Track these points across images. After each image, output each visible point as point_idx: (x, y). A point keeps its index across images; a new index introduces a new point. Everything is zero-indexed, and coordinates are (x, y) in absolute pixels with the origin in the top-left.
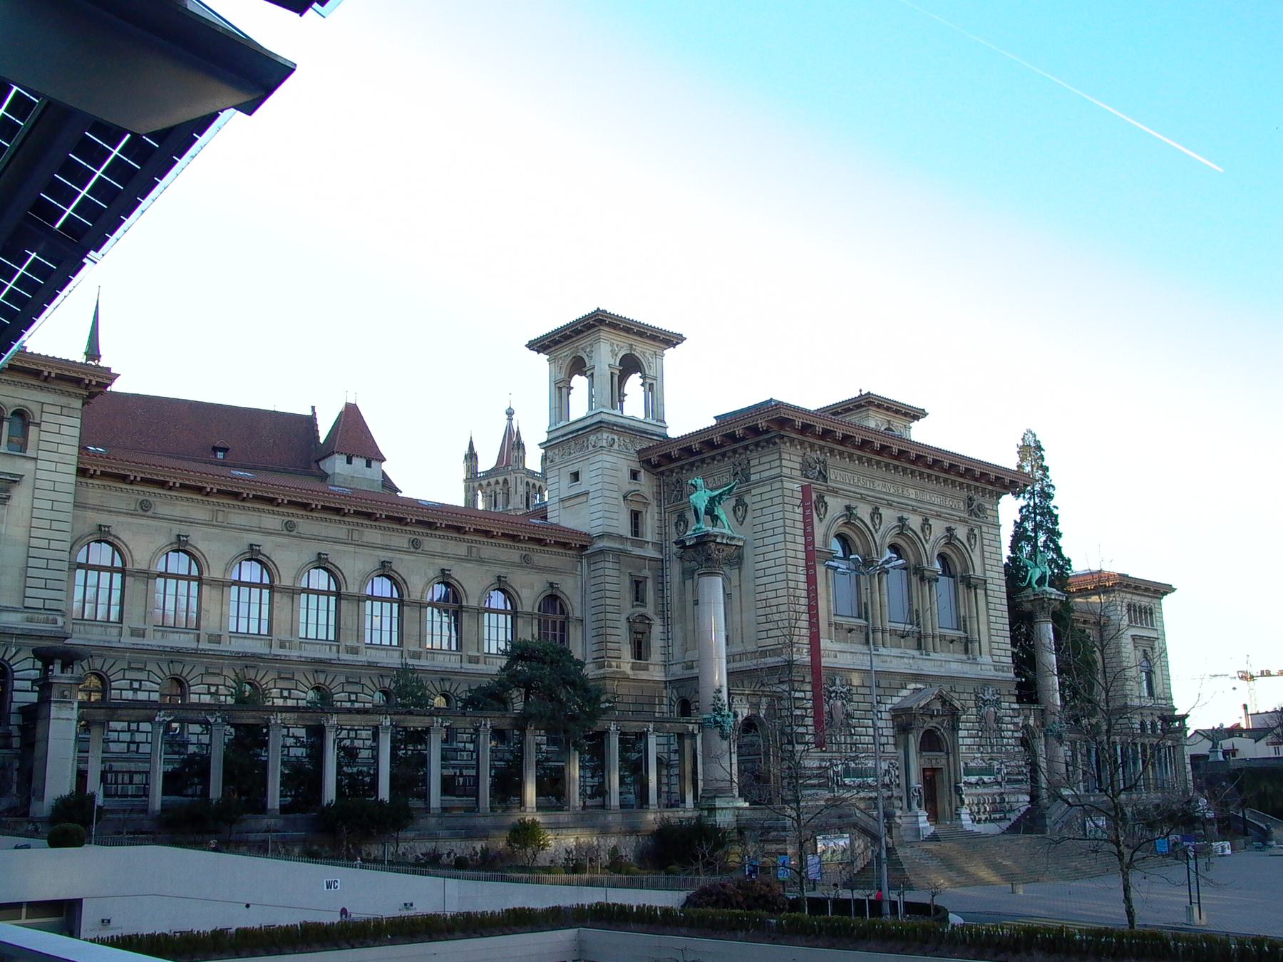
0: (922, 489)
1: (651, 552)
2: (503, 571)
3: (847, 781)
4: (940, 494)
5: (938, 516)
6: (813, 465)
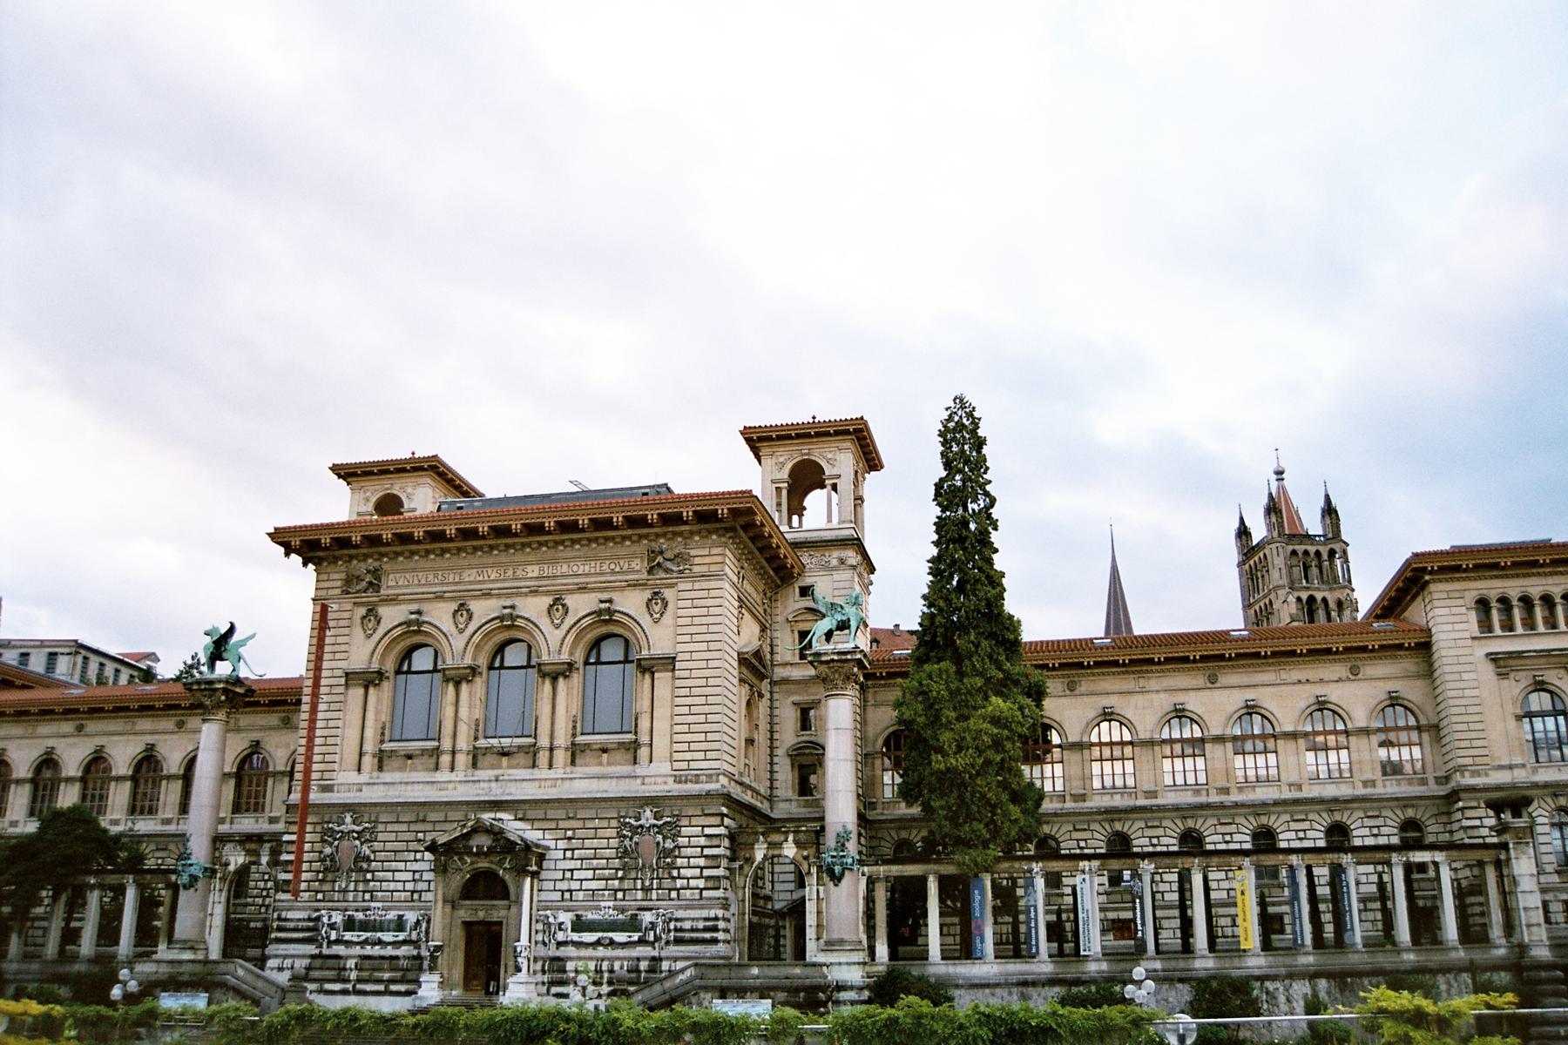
0: (554, 561)
3: (348, 936)
4: (587, 559)
5: (582, 589)
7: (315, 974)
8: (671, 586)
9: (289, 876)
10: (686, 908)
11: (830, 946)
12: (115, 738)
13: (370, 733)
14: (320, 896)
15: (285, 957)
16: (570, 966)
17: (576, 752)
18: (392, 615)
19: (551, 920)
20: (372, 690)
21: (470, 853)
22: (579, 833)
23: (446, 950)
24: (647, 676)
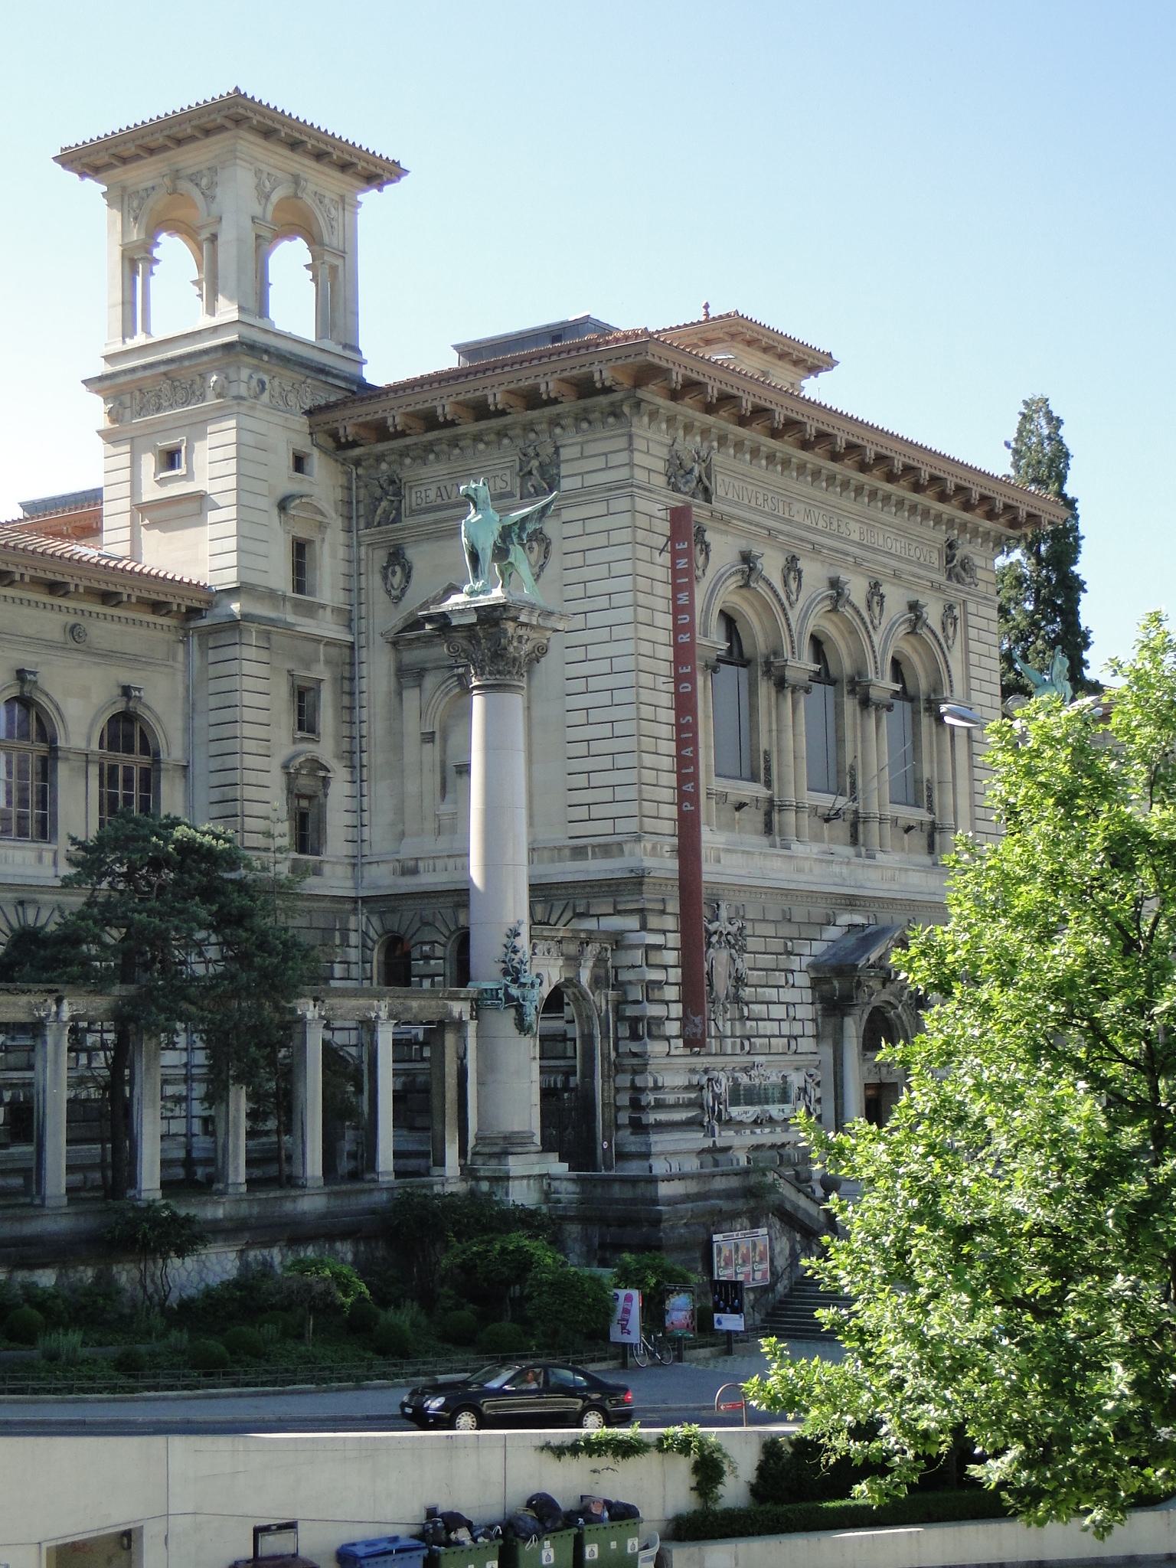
1: (329, 627)
2: (26, 659)
3: (735, 1112)
6: (689, 464)
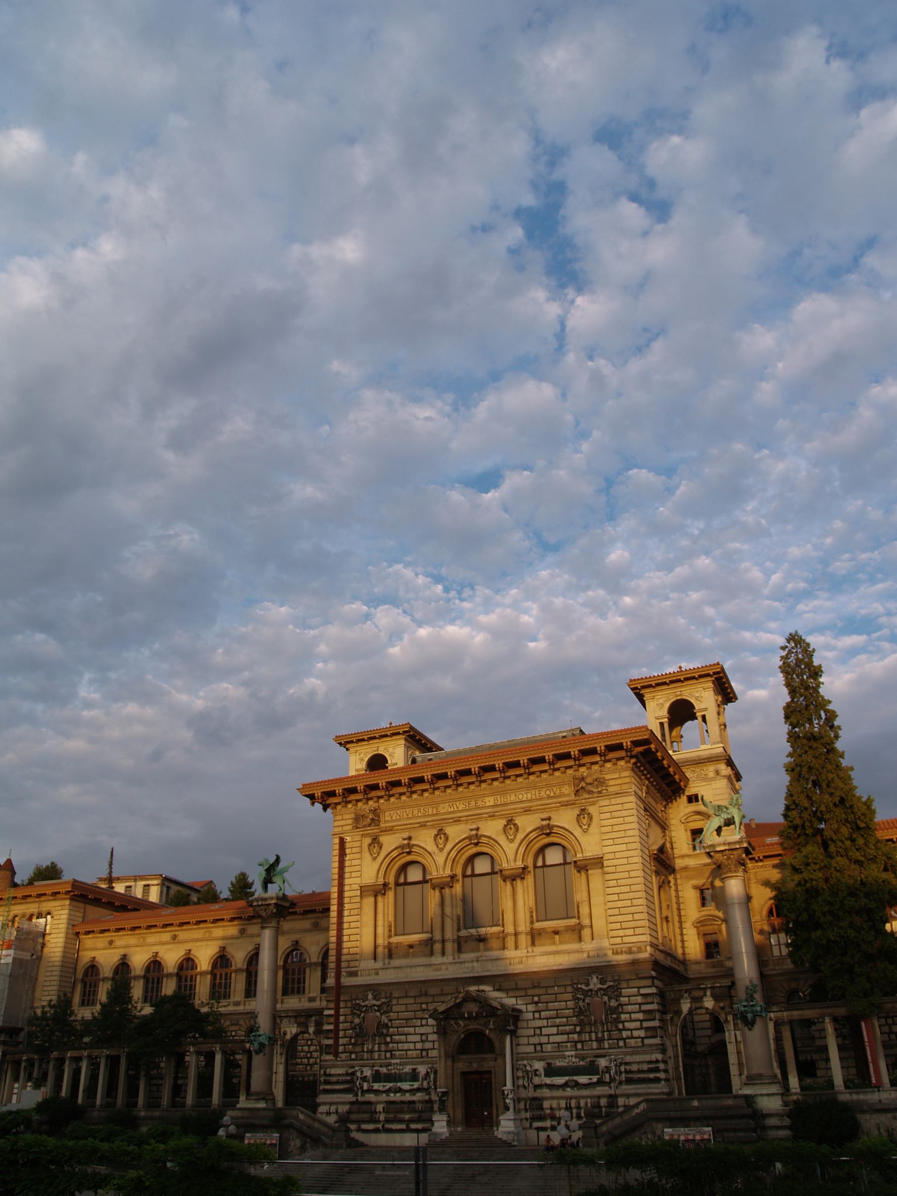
0: (504, 792)
3: (376, 1086)
4: (528, 788)
5: (527, 811)
7: (354, 1117)
8: (593, 804)
9: (331, 1042)
10: (632, 1054)
11: (751, 1080)
12: (198, 944)
13: (380, 930)
14: (353, 1056)
15: (331, 1104)
16: (546, 1104)
17: (535, 936)
18: (390, 842)
19: (528, 1068)
20: (380, 898)
21: (463, 1018)
22: (544, 998)
23: (451, 1095)
24: (583, 873)
